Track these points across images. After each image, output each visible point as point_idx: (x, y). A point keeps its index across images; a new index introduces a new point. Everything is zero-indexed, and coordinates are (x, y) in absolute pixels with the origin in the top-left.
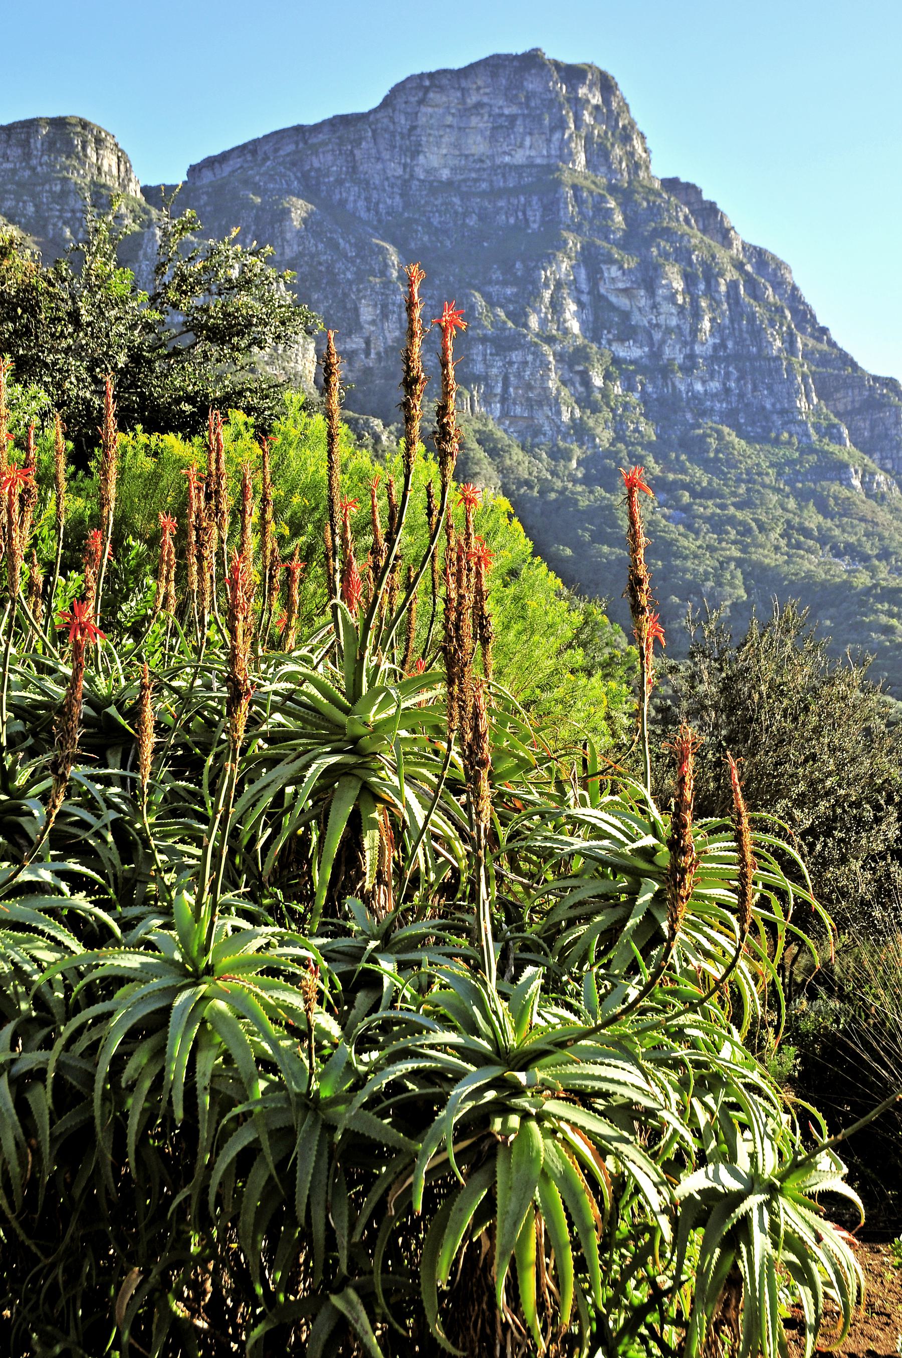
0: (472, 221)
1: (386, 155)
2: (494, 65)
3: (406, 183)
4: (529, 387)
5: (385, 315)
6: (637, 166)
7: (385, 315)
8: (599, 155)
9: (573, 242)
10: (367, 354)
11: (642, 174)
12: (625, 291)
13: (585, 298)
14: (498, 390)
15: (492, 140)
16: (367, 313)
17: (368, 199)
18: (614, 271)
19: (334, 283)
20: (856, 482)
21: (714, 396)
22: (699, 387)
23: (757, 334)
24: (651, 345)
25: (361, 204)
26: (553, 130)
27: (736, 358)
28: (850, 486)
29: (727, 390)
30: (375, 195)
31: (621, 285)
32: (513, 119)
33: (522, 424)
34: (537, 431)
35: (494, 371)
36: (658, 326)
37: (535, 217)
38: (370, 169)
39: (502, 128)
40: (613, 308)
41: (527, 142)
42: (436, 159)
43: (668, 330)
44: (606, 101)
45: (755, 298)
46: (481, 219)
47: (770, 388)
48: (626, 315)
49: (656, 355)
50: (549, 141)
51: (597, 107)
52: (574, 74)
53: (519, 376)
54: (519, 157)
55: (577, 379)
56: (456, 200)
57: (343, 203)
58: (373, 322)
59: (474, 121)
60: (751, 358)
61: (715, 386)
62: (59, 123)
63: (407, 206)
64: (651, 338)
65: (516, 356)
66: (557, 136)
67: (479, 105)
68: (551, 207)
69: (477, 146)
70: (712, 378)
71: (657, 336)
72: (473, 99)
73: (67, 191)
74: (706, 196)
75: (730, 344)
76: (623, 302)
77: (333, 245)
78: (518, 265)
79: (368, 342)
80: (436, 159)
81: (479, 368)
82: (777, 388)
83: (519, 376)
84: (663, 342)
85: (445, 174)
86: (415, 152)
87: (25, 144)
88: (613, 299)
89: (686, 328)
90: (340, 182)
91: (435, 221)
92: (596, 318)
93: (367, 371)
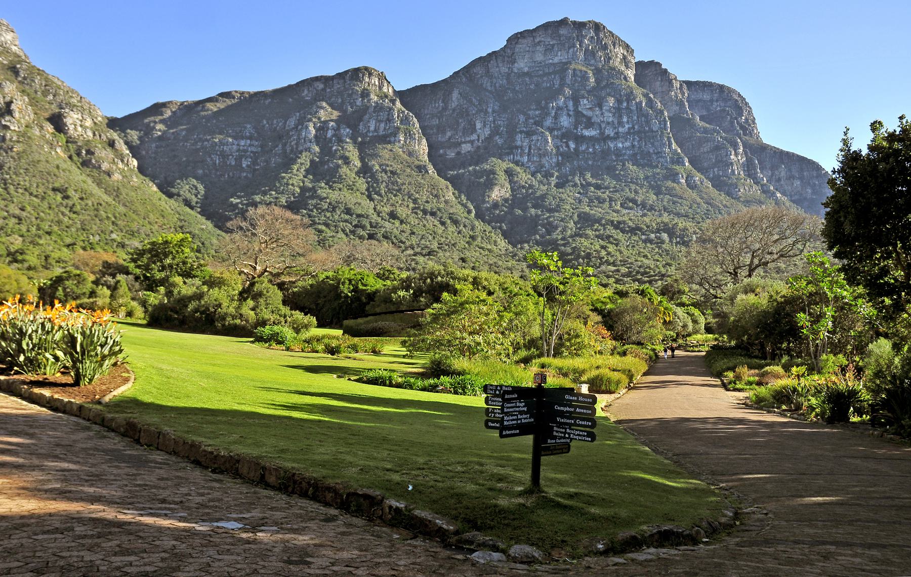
0: (532, 87)
1: (500, 65)
2: (546, 26)
3: (509, 74)
5: (485, 126)
6: (610, 58)
7: (485, 126)
8: (590, 54)
9: (567, 91)
11: (611, 62)
12: (590, 108)
13: (571, 113)
14: (527, 151)
15: (545, 54)
17: (492, 83)
18: (585, 101)
19: (468, 115)
20: (683, 181)
21: (627, 148)
22: (620, 145)
23: (648, 122)
25: (489, 84)
26: (569, 48)
27: (639, 132)
28: (679, 183)
29: (633, 146)
30: (494, 81)
32: (553, 45)
33: (537, 164)
34: (542, 166)
35: (525, 144)
37: (557, 83)
38: (494, 70)
39: (549, 49)
40: (584, 116)
41: (559, 54)
42: (522, 65)
43: (608, 123)
44: (597, 35)
45: (651, 108)
46: (536, 85)
47: (653, 144)
48: (589, 118)
49: (602, 133)
51: (592, 37)
52: (580, 26)
53: (535, 145)
54: (556, 60)
55: (564, 145)
56: (527, 79)
57: (482, 85)
59: (538, 48)
60: (645, 132)
61: (628, 144)
62: (357, 70)
63: (508, 83)
64: (600, 126)
65: (534, 138)
66: (571, 50)
68: (563, 79)
69: (539, 57)
70: (626, 141)
71: (603, 126)
73: (354, 92)
74: (663, 67)
75: (636, 127)
76: (590, 113)
77: (470, 101)
80: (522, 65)
81: (519, 143)
82: (656, 143)
83: (535, 145)
85: (526, 70)
86: (513, 62)
87: (344, 78)
88: (585, 112)
89: (616, 122)
90: (482, 77)
91: (517, 88)
92: (576, 120)
93: (478, 147)
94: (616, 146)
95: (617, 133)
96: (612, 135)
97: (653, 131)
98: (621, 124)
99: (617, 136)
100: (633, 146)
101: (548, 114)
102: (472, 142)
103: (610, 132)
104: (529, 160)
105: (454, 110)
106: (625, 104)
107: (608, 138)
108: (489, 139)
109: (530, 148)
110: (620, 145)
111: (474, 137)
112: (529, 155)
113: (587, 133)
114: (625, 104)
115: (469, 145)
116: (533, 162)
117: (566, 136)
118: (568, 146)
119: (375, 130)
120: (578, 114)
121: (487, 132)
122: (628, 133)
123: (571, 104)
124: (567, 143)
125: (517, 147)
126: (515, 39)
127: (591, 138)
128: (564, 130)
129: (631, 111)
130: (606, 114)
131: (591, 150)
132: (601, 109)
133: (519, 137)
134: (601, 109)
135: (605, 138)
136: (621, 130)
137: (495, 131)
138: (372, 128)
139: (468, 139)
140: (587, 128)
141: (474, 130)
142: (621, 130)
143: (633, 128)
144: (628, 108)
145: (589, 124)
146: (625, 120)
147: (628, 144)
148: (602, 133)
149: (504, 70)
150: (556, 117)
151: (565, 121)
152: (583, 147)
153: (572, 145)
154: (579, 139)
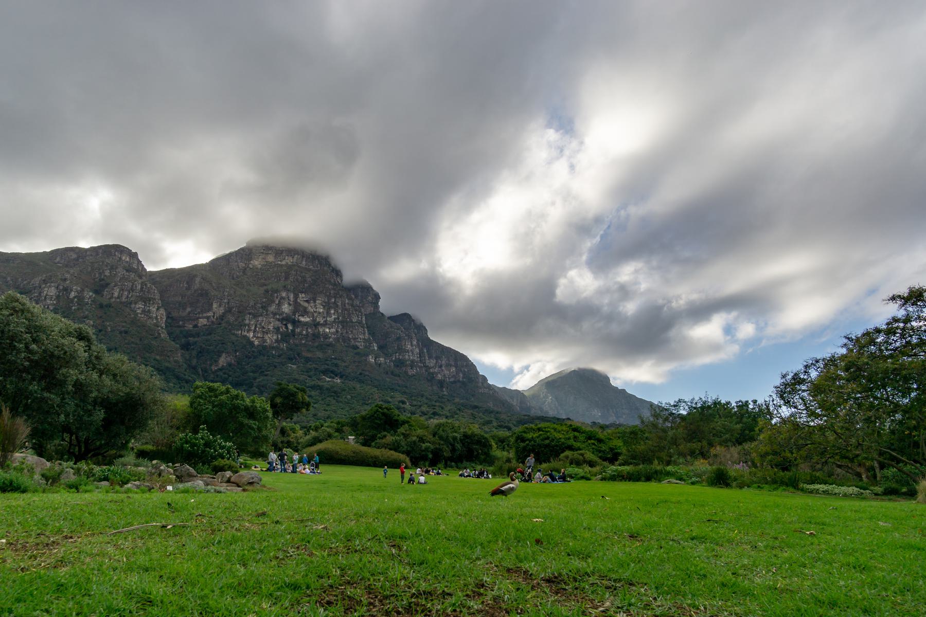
5: (220, 306)
7: (220, 306)
16: (215, 306)
21: (332, 333)
22: (327, 330)
27: (342, 322)
48: (305, 308)
49: (314, 320)
54: (284, 263)
61: (333, 330)
65: (260, 319)
71: (315, 315)
76: (306, 305)
80: (257, 263)
81: (247, 322)
93: (213, 322)
95: (326, 321)
98: (329, 314)
99: (325, 324)
100: (337, 331)
101: (274, 302)
102: (208, 318)
103: (320, 320)
104: (254, 336)
105: (195, 291)
108: (222, 317)
110: (327, 330)
111: (210, 314)
113: (302, 319)
116: (258, 338)
117: (286, 320)
118: (287, 328)
122: (334, 322)
123: (292, 296)
124: (286, 325)
125: (245, 325)
127: (306, 324)
129: (337, 306)
135: (316, 325)
137: (229, 310)
138: (116, 294)
139: (205, 315)
141: (210, 309)
144: (335, 303)
145: (305, 312)
146: (332, 312)
147: (333, 330)
148: (314, 320)
149: (242, 265)
150: (279, 305)
151: (286, 308)
152: (298, 330)
153: (290, 327)
154: (295, 323)
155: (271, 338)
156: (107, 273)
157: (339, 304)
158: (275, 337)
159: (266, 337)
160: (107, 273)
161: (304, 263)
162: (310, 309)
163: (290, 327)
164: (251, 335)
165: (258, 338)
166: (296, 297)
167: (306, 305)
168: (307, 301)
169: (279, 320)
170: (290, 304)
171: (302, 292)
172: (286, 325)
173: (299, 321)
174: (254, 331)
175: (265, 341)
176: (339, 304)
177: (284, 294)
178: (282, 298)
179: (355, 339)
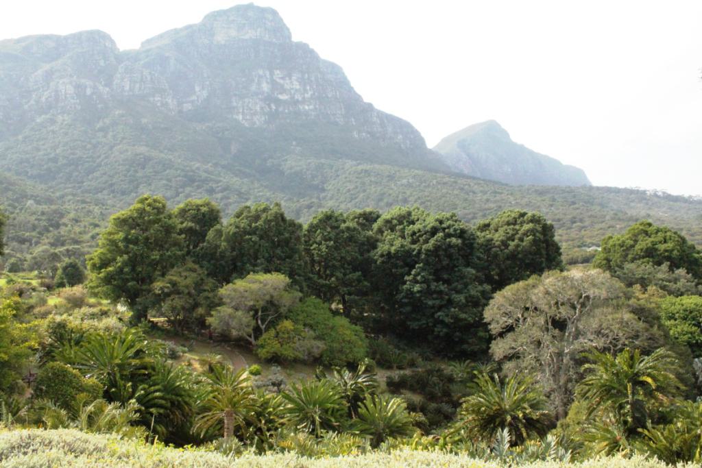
4: (251, 110)
5: (203, 88)
7: (203, 88)
10: (198, 100)
14: (241, 111)
16: (197, 89)
22: (307, 107)
24: (291, 94)
29: (316, 109)
31: (280, 76)
35: (239, 105)
36: (292, 89)
43: (296, 90)
48: (282, 86)
49: (293, 98)
50: (256, 31)
53: (247, 106)
54: (247, 37)
55: (267, 107)
58: (200, 91)
61: (311, 107)
65: (246, 100)
67: (234, 20)
69: (233, 33)
71: (293, 92)
72: (231, 18)
75: (316, 94)
76: (282, 82)
78: (247, 71)
79: (198, 97)
80: (220, 38)
81: (235, 104)
84: (294, 94)
85: (223, 42)
88: (278, 80)
94: (304, 108)
95: (304, 98)
96: (300, 99)
97: (328, 97)
98: (306, 91)
99: (304, 101)
102: (192, 102)
103: (298, 97)
104: (243, 119)
106: (306, 75)
107: (298, 101)
109: (243, 107)
110: (307, 107)
111: (194, 98)
112: (242, 115)
113: (281, 97)
114: (306, 75)
115: (190, 104)
116: (246, 120)
117: (269, 99)
119: (130, 90)
120: (273, 83)
121: (205, 94)
123: (268, 73)
124: (269, 105)
125: (234, 108)
126: (214, 16)
127: (285, 102)
128: (266, 95)
129: (311, 81)
130: (295, 83)
131: (286, 111)
132: (290, 79)
133: (234, 99)
134: (290, 79)
135: (296, 102)
136: (306, 95)
138: (127, 88)
140: (281, 93)
142: (306, 95)
143: (314, 94)
144: (308, 79)
145: (283, 91)
146: (308, 88)
147: (311, 107)
148: (293, 98)
150: (259, 84)
151: (265, 87)
152: (281, 109)
153: (273, 107)
154: (278, 102)
155: (259, 120)
156: (102, 63)
157: (313, 79)
158: (263, 119)
159: (255, 119)
160: (102, 63)
161: (267, 36)
162: (287, 87)
163: (273, 107)
164: (240, 117)
165: (246, 120)
166: (272, 74)
167: (282, 82)
168: (282, 78)
169: (261, 100)
170: (267, 83)
171: (277, 69)
172: (269, 105)
173: (279, 100)
174: (243, 113)
175: (255, 123)
176: (313, 79)
177: (261, 72)
178: (260, 77)
179: (334, 115)
